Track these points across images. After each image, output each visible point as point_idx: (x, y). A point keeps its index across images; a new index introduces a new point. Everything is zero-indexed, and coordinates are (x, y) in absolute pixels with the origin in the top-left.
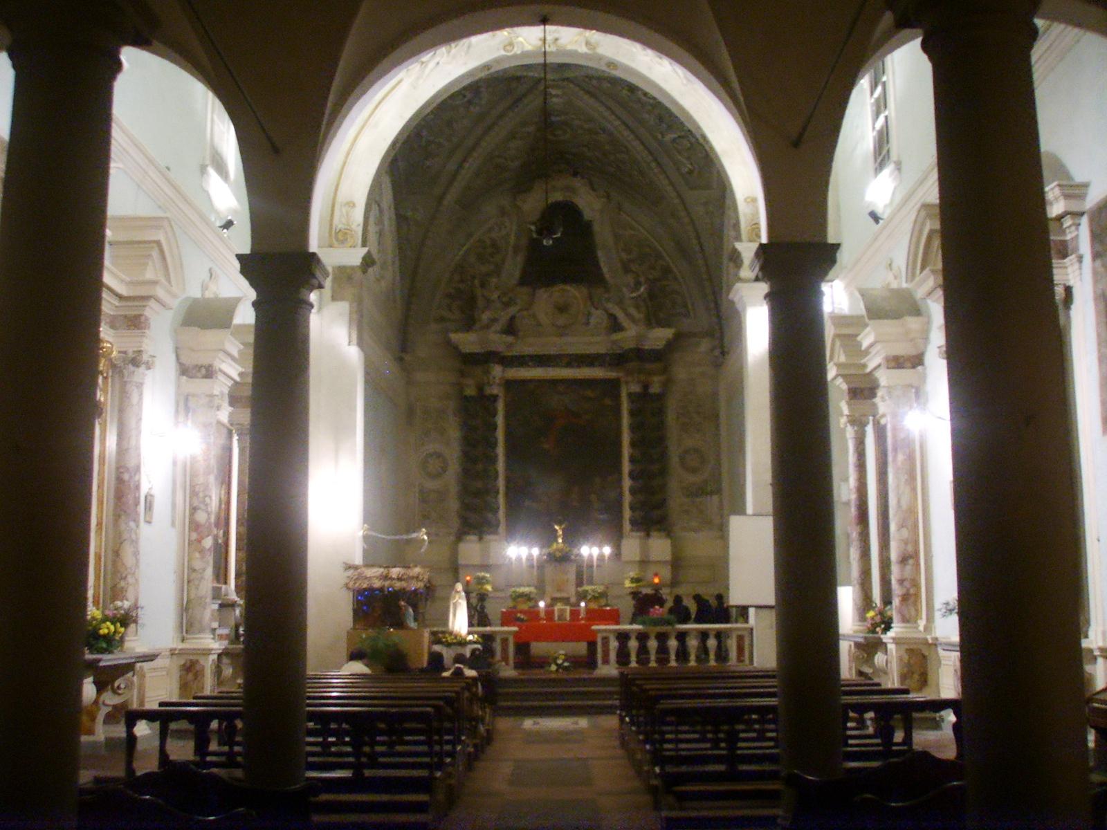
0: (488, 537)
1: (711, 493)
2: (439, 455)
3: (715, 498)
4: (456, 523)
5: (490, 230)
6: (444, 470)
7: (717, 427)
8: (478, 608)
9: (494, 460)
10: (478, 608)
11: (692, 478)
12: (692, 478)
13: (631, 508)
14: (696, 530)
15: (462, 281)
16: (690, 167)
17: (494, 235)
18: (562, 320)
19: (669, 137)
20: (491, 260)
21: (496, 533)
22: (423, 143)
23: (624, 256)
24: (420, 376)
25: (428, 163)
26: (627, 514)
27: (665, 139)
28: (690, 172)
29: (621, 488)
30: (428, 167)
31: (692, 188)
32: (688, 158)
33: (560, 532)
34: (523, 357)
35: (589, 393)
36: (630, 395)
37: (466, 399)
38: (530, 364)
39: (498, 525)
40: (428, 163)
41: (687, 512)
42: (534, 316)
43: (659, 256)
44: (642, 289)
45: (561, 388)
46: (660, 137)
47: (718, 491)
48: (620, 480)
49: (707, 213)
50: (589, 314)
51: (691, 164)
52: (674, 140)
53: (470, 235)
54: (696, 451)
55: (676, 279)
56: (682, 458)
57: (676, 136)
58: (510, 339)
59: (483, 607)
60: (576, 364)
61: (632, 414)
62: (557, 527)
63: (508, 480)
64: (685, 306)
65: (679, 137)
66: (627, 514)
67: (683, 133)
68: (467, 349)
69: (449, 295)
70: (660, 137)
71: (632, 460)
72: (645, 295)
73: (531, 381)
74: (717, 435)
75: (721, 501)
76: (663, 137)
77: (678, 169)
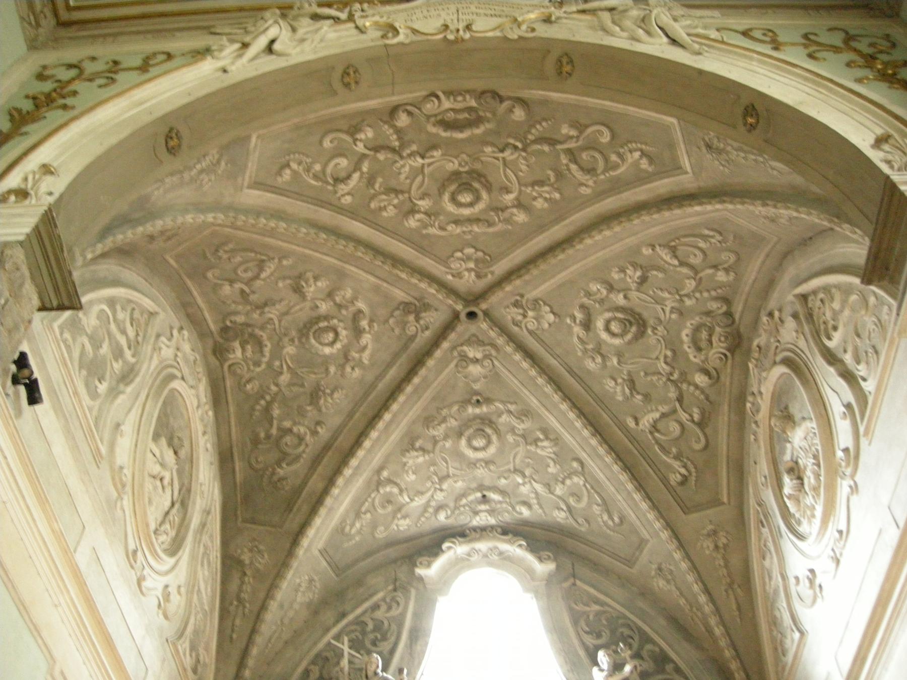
5: (376, 607)
16: (683, 471)
17: (380, 614)
19: (647, 420)
20: (373, 648)
22: (274, 431)
23: (590, 641)
25: (281, 472)
27: (641, 426)
28: (685, 481)
30: (281, 479)
31: (686, 510)
32: (677, 457)
40: (281, 472)
43: (646, 639)
44: (628, 668)
46: (631, 423)
49: (717, 547)
51: (685, 467)
52: (655, 427)
53: (343, 615)
55: (678, 670)
57: (657, 415)
65: (664, 415)
67: (664, 409)
70: (631, 423)
76: (637, 424)
77: (665, 481)
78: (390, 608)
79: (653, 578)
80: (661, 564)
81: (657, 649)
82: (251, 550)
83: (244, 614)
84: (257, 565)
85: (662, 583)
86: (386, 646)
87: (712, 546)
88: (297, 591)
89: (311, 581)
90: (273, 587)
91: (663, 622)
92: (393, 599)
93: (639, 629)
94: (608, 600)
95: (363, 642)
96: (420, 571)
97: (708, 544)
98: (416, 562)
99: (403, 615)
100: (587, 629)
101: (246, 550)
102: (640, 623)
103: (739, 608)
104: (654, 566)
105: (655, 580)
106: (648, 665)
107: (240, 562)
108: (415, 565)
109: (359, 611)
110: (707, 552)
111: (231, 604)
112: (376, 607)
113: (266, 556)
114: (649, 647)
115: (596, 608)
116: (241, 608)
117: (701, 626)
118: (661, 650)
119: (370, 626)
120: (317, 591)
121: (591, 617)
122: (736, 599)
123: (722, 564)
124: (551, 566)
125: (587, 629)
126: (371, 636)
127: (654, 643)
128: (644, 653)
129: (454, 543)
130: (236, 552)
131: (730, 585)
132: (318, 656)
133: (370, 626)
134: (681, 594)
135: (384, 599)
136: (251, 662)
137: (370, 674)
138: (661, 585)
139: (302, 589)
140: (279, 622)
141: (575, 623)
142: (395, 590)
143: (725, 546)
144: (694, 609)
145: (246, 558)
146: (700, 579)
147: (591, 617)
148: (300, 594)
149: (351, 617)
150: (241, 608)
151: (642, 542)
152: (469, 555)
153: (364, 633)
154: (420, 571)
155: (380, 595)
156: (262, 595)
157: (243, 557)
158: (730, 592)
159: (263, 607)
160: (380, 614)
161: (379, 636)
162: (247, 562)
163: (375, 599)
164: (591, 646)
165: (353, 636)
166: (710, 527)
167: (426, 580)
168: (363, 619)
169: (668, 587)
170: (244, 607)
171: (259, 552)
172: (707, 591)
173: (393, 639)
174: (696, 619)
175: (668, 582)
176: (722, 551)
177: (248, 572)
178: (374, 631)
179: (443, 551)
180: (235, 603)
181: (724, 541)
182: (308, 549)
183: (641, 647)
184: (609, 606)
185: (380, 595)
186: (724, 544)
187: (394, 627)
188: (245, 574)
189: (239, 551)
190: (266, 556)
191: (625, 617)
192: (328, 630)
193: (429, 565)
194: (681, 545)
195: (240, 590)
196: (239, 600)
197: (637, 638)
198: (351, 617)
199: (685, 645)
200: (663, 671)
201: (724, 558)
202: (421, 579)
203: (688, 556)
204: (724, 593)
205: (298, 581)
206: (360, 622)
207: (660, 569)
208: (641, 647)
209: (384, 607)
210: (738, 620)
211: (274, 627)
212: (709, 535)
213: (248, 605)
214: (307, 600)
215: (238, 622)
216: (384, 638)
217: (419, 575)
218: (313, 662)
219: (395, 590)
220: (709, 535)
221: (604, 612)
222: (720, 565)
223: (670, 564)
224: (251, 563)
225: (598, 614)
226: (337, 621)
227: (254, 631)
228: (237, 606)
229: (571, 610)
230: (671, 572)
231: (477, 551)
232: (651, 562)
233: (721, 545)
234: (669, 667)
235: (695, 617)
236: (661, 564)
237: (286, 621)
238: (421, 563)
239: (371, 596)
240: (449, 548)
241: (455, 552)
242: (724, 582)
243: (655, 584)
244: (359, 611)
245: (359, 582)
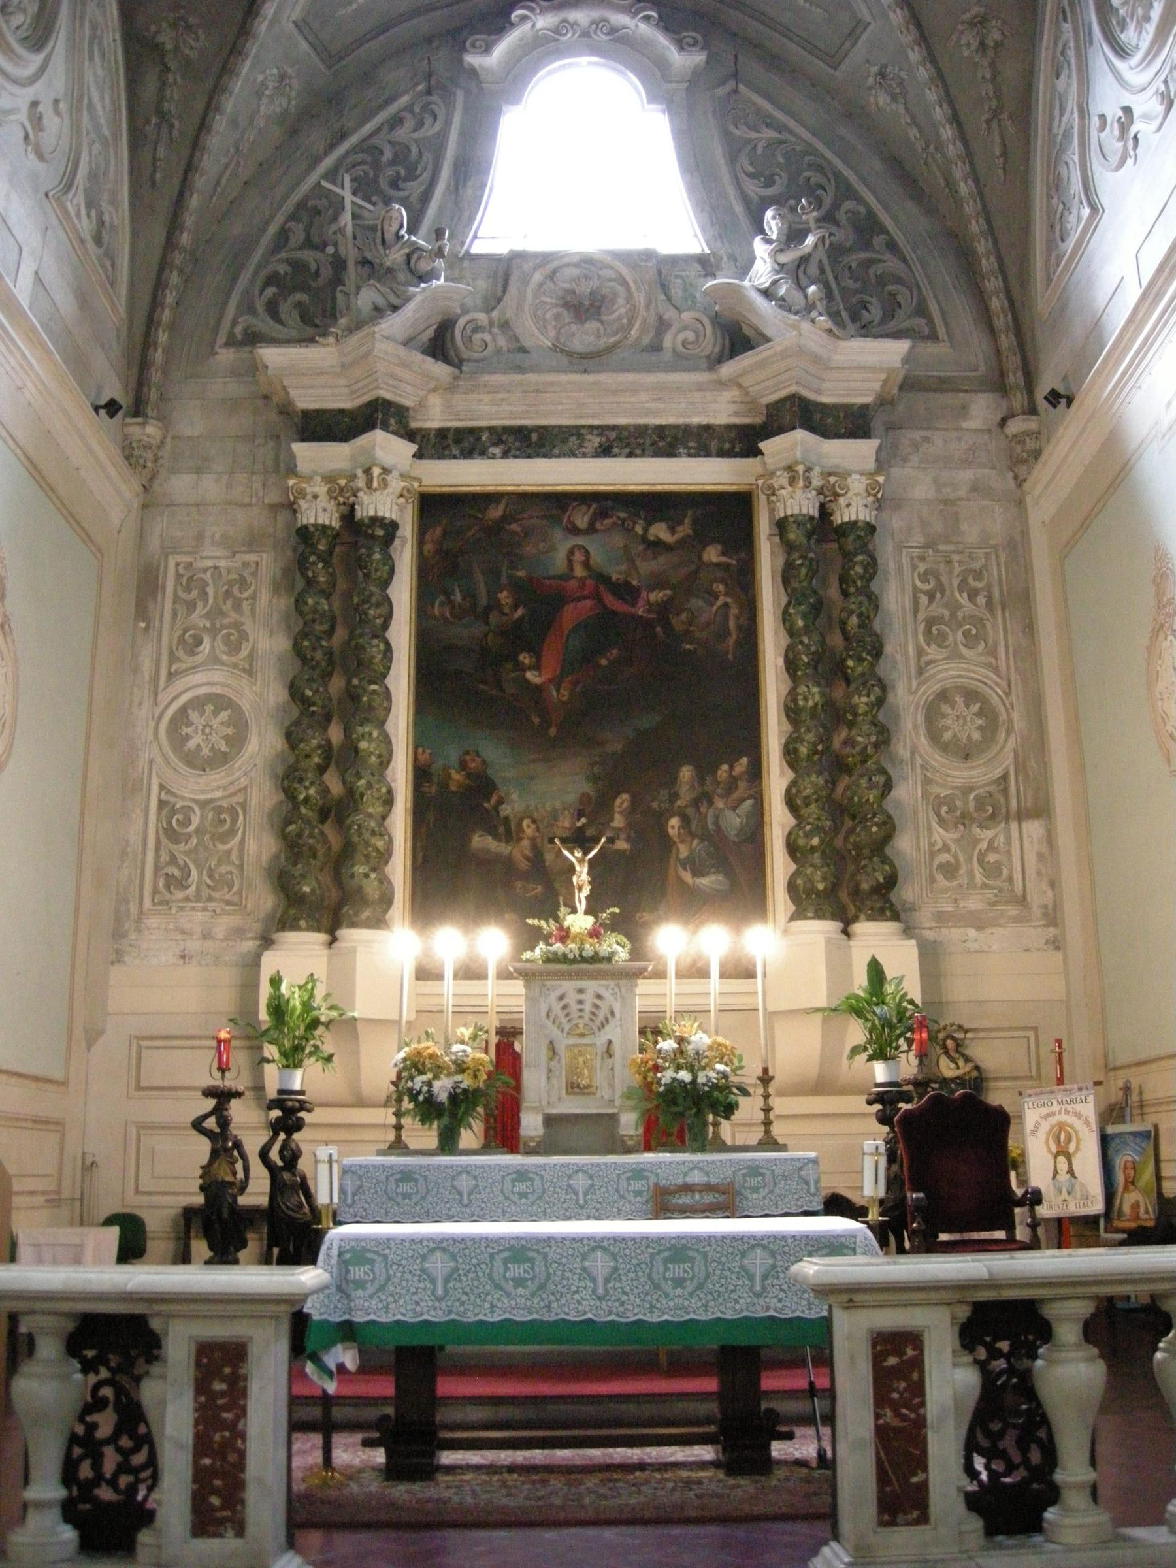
0: (351, 936)
1: (1022, 815)
2: (220, 702)
3: (1034, 829)
4: (265, 900)
5: (396, 122)
6: (237, 740)
7: (1030, 628)
8: (274, 1154)
9: (378, 712)
10: (274, 1154)
11: (959, 774)
12: (959, 774)
13: (793, 849)
14: (979, 922)
15: (308, 244)
18: (584, 337)
20: (394, 193)
21: (379, 922)
23: (754, 189)
24: (180, 485)
26: (780, 867)
29: (759, 799)
33: (582, 875)
34: (473, 432)
35: (660, 531)
36: (781, 526)
37: (305, 534)
38: (497, 451)
39: (387, 901)
41: (949, 870)
42: (505, 325)
43: (847, 192)
44: (810, 240)
45: (582, 520)
47: (1041, 810)
48: (756, 773)
49: (983, 45)
50: (662, 325)
53: (343, 136)
54: (971, 696)
55: (892, 246)
56: (932, 714)
58: (440, 370)
59: (291, 1157)
60: (627, 450)
61: (787, 576)
62: (573, 856)
63: (421, 774)
64: (922, 310)
66: (780, 867)
68: (306, 400)
69: (272, 280)
71: (792, 712)
72: (821, 254)
73: (486, 499)
74: (1029, 656)
75: (1050, 839)
78: (420, 125)
79: (870, 88)
80: (885, 66)
81: (862, 210)
82: (174, 26)
83: (171, 138)
84: (187, 51)
85: (883, 99)
86: (414, 189)
87: (975, 44)
88: (259, 94)
89: (282, 77)
90: (217, 89)
91: (878, 165)
92: (425, 107)
93: (837, 175)
94: (792, 124)
95: (376, 181)
96: (472, 59)
97: (970, 39)
98: (464, 42)
99: (443, 135)
100: (751, 169)
101: (164, 25)
102: (839, 164)
103: (1004, 153)
104: (875, 69)
105: (873, 92)
106: (844, 235)
107: (158, 48)
108: (463, 49)
109: (368, 128)
110: (966, 54)
111: (148, 122)
112: (396, 122)
113: (202, 36)
114: (849, 205)
115: (772, 134)
116: (165, 129)
117: (938, 174)
118: (871, 214)
119: (388, 155)
120: (293, 94)
121: (759, 150)
122: (1002, 135)
123: (988, 76)
124: (698, 58)
125: (751, 169)
126: (390, 172)
127: (859, 199)
128: (841, 216)
129: (532, 10)
130: (148, 29)
131: (996, 113)
132: (302, 205)
133: (388, 155)
134: (913, 117)
135: (409, 108)
136: (189, 220)
137: (389, 237)
138: (881, 103)
139: (267, 92)
140: (232, 150)
141: (732, 159)
142: (429, 92)
143: (998, 45)
144: (932, 148)
145: (166, 38)
146: (949, 99)
147: (759, 150)
148: (264, 100)
149: (353, 140)
150: (165, 129)
151: (858, 27)
152: (557, 30)
153: (377, 166)
154: (472, 59)
155: (404, 100)
156: (200, 105)
157: (160, 39)
158: (995, 124)
159: (203, 126)
160: (402, 133)
161: (403, 172)
162: (169, 46)
163: (393, 108)
164: (756, 198)
165: (358, 172)
166: (976, 10)
167: (482, 76)
168: (374, 141)
169: (894, 107)
170: (172, 126)
171: (189, 28)
172: (956, 119)
173: (426, 176)
174: (934, 167)
175: (894, 98)
176: (991, 53)
177: (172, 65)
178: (394, 162)
179: (512, 25)
180: (154, 120)
181: (996, 35)
182: (275, 21)
183: (836, 206)
184: (791, 132)
185: (404, 100)
186: (996, 43)
187: (427, 156)
188: (168, 69)
189: (153, 28)
190: (202, 36)
191: (815, 152)
192: (317, 160)
193: (487, 50)
194: (923, 38)
195: (161, 98)
196: (163, 116)
197: (831, 188)
198: (353, 140)
199: (910, 205)
200: (867, 245)
201: (992, 64)
202: (473, 73)
203: (932, 58)
204: (984, 126)
205: (260, 78)
206: (368, 148)
207: (882, 75)
208: (836, 206)
209: (409, 123)
210: (1001, 172)
211: (224, 160)
212: (972, 24)
213: (176, 123)
214: (278, 110)
215: (162, 153)
216: (412, 175)
217: (469, 64)
218: (293, 217)
219: (429, 92)
220: (972, 24)
221: (782, 142)
222: (983, 77)
223: (901, 69)
224: (177, 48)
225: (771, 145)
226: (332, 146)
227: (190, 168)
228: (158, 126)
229: (726, 135)
230: (901, 83)
231: (574, 25)
232: (868, 61)
233: (992, 44)
234: (879, 241)
235: (930, 160)
236: (885, 66)
237: (244, 147)
238: (473, 46)
239: (388, 102)
240: (524, 18)
241: (533, 26)
242: (987, 107)
243: (872, 99)
244: (368, 128)
245: (367, 77)
